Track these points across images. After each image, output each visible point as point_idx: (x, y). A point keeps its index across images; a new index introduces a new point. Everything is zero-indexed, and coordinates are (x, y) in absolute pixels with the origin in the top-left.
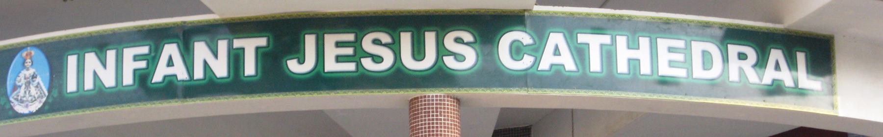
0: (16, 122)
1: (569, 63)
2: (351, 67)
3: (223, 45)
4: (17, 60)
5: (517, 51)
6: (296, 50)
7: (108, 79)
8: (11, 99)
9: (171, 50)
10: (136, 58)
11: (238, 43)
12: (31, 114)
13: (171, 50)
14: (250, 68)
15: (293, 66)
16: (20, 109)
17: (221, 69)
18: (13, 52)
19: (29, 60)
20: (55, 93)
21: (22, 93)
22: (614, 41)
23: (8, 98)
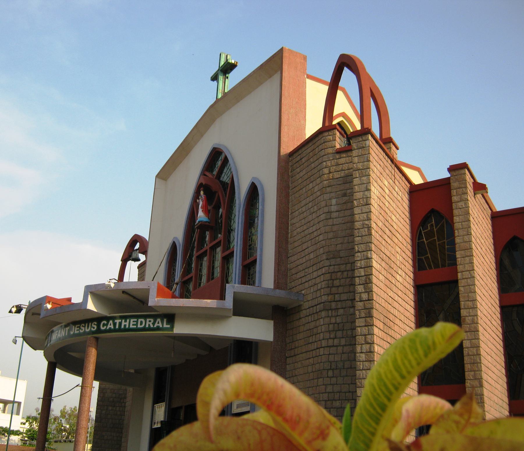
5: (104, 325)
22: (122, 321)
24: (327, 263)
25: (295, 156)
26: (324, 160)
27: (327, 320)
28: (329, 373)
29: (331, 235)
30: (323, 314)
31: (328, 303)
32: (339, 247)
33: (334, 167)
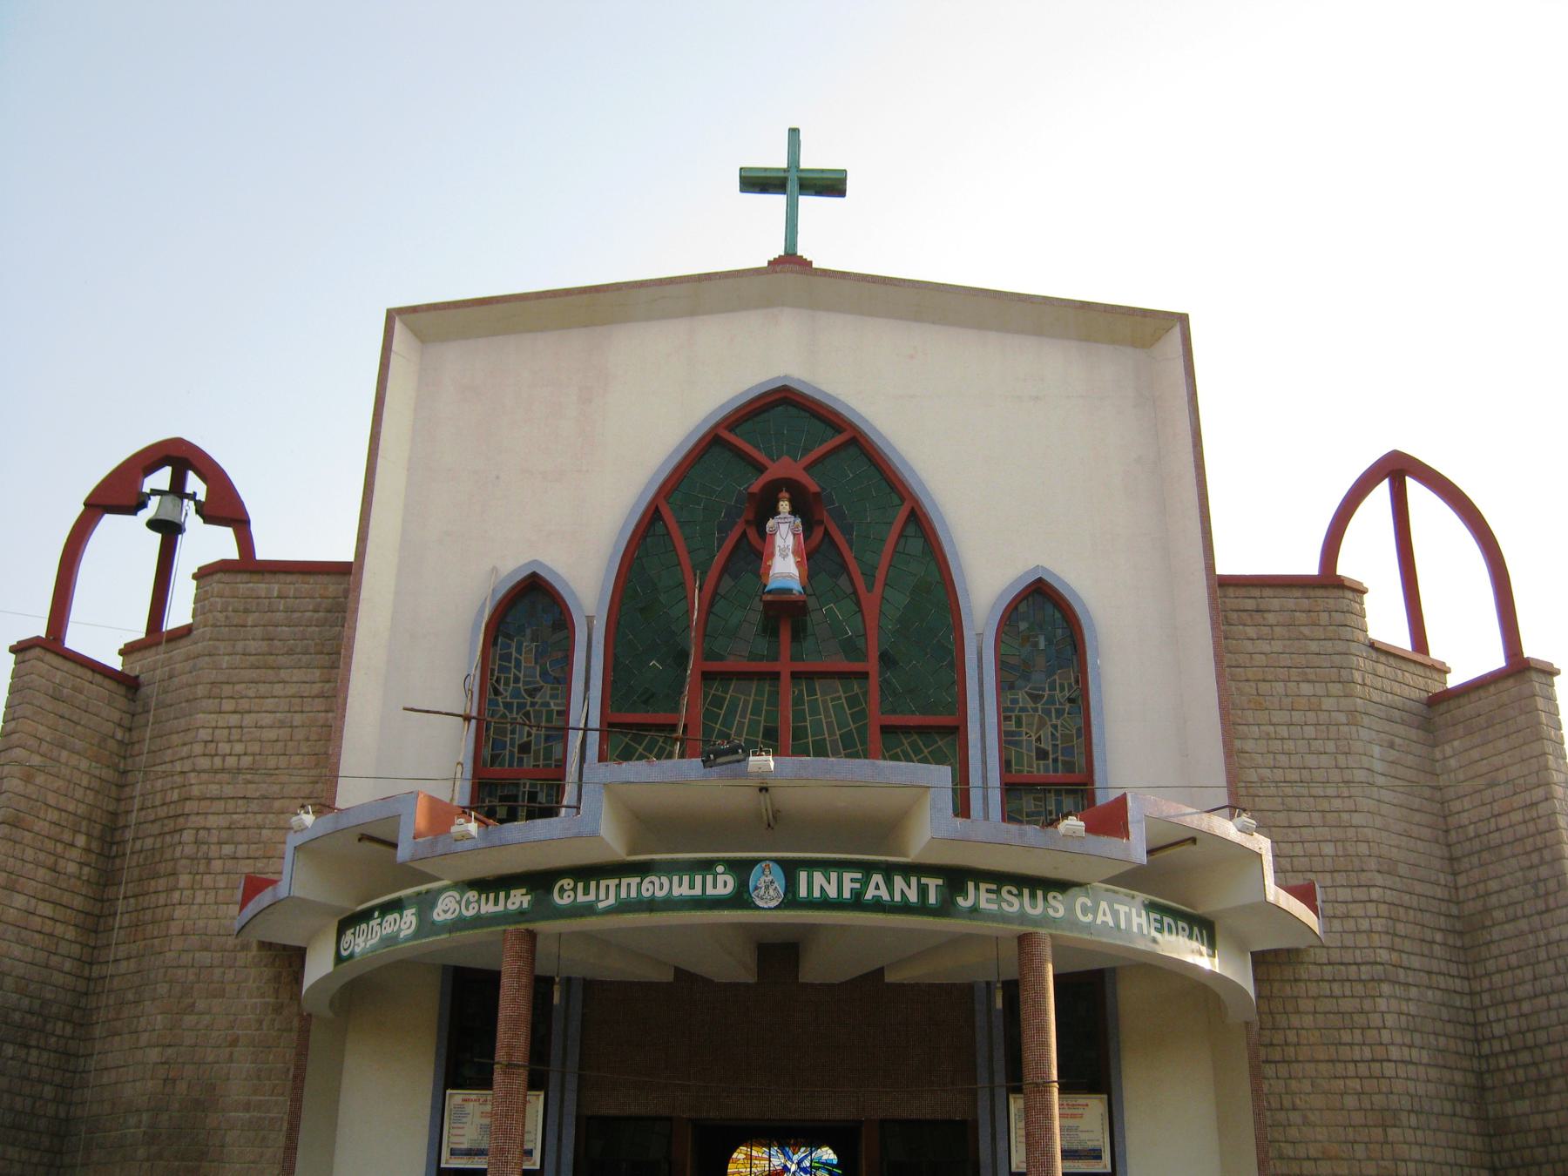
0: (757, 912)
1: (1109, 920)
2: (994, 907)
3: (914, 880)
4: (757, 867)
5: (1085, 911)
6: (963, 891)
7: (832, 892)
8: (753, 895)
9: (877, 878)
10: (853, 880)
11: (923, 880)
12: (770, 909)
13: (877, 878)
14: (932, 899)
15: (960, 900)
16: (760, 903)
17: (913, 897)
18: (753, 863)
19: (767, 870)
20: (790, 896)
21: (762, 893)
22: (1130, 910)
23: (750, 894)
24: (1379, 880)
25: (1231, 592)
26: (1353, 651)
27: (1394, 1004)
28: (1411, 1119)
29: (1379, 822)
30: (1386, 988)
31: (1390, 967)
32: (1395, 853)
33: (1370, 676)
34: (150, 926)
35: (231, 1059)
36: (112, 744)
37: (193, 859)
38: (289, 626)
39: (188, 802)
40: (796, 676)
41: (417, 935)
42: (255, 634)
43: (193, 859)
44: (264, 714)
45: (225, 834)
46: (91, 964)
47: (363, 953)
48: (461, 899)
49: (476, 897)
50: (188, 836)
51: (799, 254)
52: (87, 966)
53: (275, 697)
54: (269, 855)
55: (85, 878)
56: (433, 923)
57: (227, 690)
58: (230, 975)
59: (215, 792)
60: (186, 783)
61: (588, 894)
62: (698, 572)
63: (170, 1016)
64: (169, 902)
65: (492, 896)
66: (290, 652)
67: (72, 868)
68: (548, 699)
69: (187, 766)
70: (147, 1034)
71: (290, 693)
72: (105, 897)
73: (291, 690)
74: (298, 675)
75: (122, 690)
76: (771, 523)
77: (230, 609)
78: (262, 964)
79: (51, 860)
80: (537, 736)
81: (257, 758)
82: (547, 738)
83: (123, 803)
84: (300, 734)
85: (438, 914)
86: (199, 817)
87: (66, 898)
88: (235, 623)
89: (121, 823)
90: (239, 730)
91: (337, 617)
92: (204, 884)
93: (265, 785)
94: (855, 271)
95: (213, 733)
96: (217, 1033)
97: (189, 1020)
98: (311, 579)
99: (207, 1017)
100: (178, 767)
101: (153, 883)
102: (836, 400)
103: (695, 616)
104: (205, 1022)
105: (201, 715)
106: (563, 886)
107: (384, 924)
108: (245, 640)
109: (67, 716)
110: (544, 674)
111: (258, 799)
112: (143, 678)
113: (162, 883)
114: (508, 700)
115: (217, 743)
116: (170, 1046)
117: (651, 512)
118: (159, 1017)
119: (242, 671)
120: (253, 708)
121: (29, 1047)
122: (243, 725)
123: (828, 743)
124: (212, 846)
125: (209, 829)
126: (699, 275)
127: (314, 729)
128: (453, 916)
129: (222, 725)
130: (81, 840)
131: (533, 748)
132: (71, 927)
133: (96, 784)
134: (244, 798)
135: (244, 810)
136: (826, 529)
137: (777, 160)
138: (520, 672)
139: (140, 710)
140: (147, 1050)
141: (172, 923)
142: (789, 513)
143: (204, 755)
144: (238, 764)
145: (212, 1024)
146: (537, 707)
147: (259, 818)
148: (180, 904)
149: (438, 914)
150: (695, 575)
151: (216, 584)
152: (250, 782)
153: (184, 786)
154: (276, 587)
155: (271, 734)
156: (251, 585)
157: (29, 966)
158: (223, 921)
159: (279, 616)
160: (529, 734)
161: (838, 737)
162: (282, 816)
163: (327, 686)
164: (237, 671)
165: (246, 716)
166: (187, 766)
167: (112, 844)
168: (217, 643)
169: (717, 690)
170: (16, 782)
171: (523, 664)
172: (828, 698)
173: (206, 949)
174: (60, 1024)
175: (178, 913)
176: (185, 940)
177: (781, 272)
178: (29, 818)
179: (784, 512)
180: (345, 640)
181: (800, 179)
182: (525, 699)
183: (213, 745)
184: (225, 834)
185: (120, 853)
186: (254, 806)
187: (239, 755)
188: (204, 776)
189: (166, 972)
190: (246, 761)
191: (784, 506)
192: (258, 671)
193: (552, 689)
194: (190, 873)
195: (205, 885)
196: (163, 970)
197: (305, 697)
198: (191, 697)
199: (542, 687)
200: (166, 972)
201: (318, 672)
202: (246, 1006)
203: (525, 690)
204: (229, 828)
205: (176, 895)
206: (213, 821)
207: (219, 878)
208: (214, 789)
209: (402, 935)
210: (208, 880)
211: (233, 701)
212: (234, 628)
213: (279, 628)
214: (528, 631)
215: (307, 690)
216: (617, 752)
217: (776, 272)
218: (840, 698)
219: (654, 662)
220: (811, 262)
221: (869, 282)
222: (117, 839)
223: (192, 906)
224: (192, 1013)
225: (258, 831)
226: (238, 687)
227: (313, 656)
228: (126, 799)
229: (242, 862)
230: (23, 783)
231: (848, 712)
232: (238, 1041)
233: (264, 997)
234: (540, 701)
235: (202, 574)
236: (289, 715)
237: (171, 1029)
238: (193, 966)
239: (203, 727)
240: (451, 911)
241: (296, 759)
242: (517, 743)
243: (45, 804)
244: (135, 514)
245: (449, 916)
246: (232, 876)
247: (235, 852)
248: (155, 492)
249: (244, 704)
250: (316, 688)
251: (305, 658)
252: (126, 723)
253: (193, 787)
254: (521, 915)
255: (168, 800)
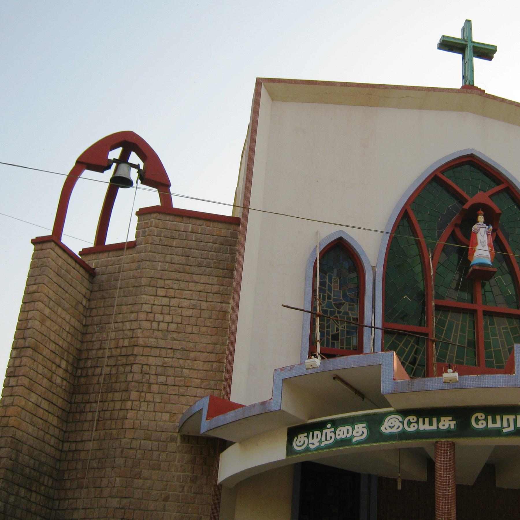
34: (109, 422)
35: (164, 510)
36: (81, 308)
37: (139, 383)
38: (199, 250)
39: (136, 348)
40: (486, 313)
41: (367, 440)
42: (178, 252)
43: (139, 383)
44: (184, 300)
45: (160, 370)
46: (63, 442)
47: (318, 449)
48: (404, 421)
49: (484, 417)
50: (136, 368)
51: (475, 85)
52: (61, 443)
53: (190, 290)
54: (187, 385)
55: (64, 388)
56: (381, 434)
57: (161, 283)
58: (164, 456)
59: (153, 343)
60: (134, 336)
61: (496, 423)
62: (430, 249)
63: (126, 479)
64: (123, 407)
65: (427, 420)
66: (199, 265)
67: (59, 380)
68: (347, 310)
69: (135, 325)
70: (108, 489)
71: (198, 289)
72: (73, 401)
73: (200, 287)
74: (204, 279)
75: (87, 276)
76: (475, 227)
77: (162, 235)
78: (184, 451)
79: (49, 375)
80: (342, 331)
81: (179, 325)
82: (348, 333)
83: (86, 344)
84: (206, 314)
85: (385, 428)
86: (143, 358)
87: (55, 399)
88: (165, 244)
89: (84, 355)
90: (168, 308)
91: (227, 249)
92: (146, 398)
93: (184, 342)
94: (509, 99)
95: (152, 307)
96: (155, 492)
97: (138, 482)
98: (212, 224)
99: (149, 481)
100: (128, 326)
101: (110, 395)
102: (499, 165)
103: (432, 274)
104: (148, 485)
105: (144, 296)
106: (409, 420)
107: (337, 432)
108: (171, 255)
109: (62, 287)
110: (345, 296)
111: (180, 350)
112: (97, 270)
113: (117, 396)
114: (325, 308)
115: (155, 314)
116: (125, 498)
117: (404, 211)
118: (118, 479)
119: (170, 273)
120: (177, 295)
121: (31, 491)
122: (171, 305)
123: (502, 352)
124: (151, 376)
125: (150, 366)
126: (428, 88)
127: (215, 312)
128: (398, 430)
129: (157, 304)
130: (64, 364)
131: (340, 338)
132: (55, 418)
133: (72, 331)
134: (172, 349)
135: (171, 356)
136: (497, 233)
137: (457, 34)
138: (331, 293)
139: (96, 288)
140: (109, 499)
141: (125, 421)
142: (484, 223)
143: (146, 320)
144: (168, 328)
145: (153, 486)
146: (341, 315)
147: (181, 361)
148: (131, 409)
149: (385, 428)
150: (428, 250)
151: (153, 219)
152: (175, 340)
153: (132, 337)
154: (191, 226)
155: (189, 312)
156: (175, 223)
157: (35, 439)
158: (159, 423)
159: (193, 243)
160: (338, 330)
161: (507, 349)
162: (196, 362)
163: (222, 287)
164: (167, 272)
165: (172, 300)
166: (135, 325)
167: (77, 368)
168: (155, 254)
169: (441, 316)
170: (37, 323)
171: (333, 289)
172: (501, 327)
173: (149, 439)
174: (47, 478)
175: (131, 414)
176: (135, 432)
177: (471, 93)
178: (42, 346)
179: (482, 222)
180: (238, 262)
181: (474, 46)
182: (335, 309)
183: (152, 315)
184: (160, 370)
185: (84, 375)
186: (178, 354)
187: (168, 323)
188: (146, 333)
189: (122, 451)
190: (173, 327)
191: (481, 219)
192: (180, 274)
193: (350, 305)
194: (138, 391)
195: (147, 399)
196: (119, 451)
197: (209, 293)
198: (137, 285)
199: (344, 303)
200: (122, 451)
201: (216, 279)
202: (174, 477)
203: (334, 304)
204: (162, 366)
205: (129, 404)
206: (152, 361)
207: (156, 396)
208: (152, 342)
209: (355, 440)
210: (149, 396)
211: (165, 290)
212: (165, 247)
213: (192, 250)
214: (335, 271)
215: (209, 288)
216: (388, 345)
217: (468, 93)
218: (506, 328)
219: (406, 296)
220: (484, 91)
221: (516, 106)
222: (82, 366)
223: (139, 412)
224: (139, 478)
225: (180, 370)
226: (167, 282)
227: (213, 269)
228: (87, 342)
229: (170, 387)
230: (40, 324)
231: (512, 336)
232: (169, 498)
233: (185, 472)
234: (343, 311)
235: (142, 213)
236: (199, 302)
237: (126, 487)
238: (140, 449)
239: (145, 303)
240: (396, 427)
241: (204, 329)
242: (331, 334)
243: (49, 339)
244: (103, 172)
245: (394, 430)
246: (164, 395)
247: (166, 381)
248: (115, 160)
249: (171, 293)
250: (216, 288)
251: (208, 270)
252: (88, 296)
253: (139, 338)
254: (448, 433)
255: (120, 345)
